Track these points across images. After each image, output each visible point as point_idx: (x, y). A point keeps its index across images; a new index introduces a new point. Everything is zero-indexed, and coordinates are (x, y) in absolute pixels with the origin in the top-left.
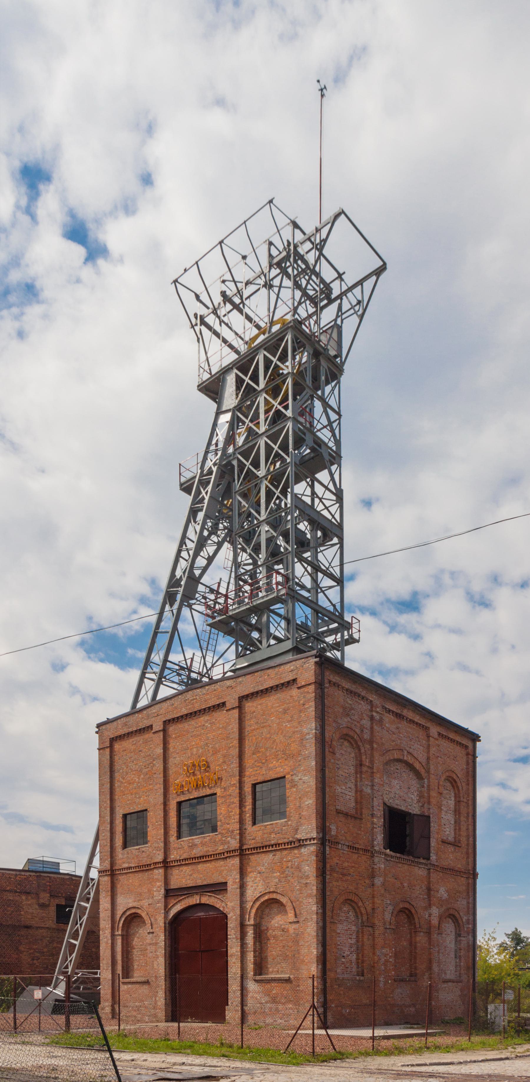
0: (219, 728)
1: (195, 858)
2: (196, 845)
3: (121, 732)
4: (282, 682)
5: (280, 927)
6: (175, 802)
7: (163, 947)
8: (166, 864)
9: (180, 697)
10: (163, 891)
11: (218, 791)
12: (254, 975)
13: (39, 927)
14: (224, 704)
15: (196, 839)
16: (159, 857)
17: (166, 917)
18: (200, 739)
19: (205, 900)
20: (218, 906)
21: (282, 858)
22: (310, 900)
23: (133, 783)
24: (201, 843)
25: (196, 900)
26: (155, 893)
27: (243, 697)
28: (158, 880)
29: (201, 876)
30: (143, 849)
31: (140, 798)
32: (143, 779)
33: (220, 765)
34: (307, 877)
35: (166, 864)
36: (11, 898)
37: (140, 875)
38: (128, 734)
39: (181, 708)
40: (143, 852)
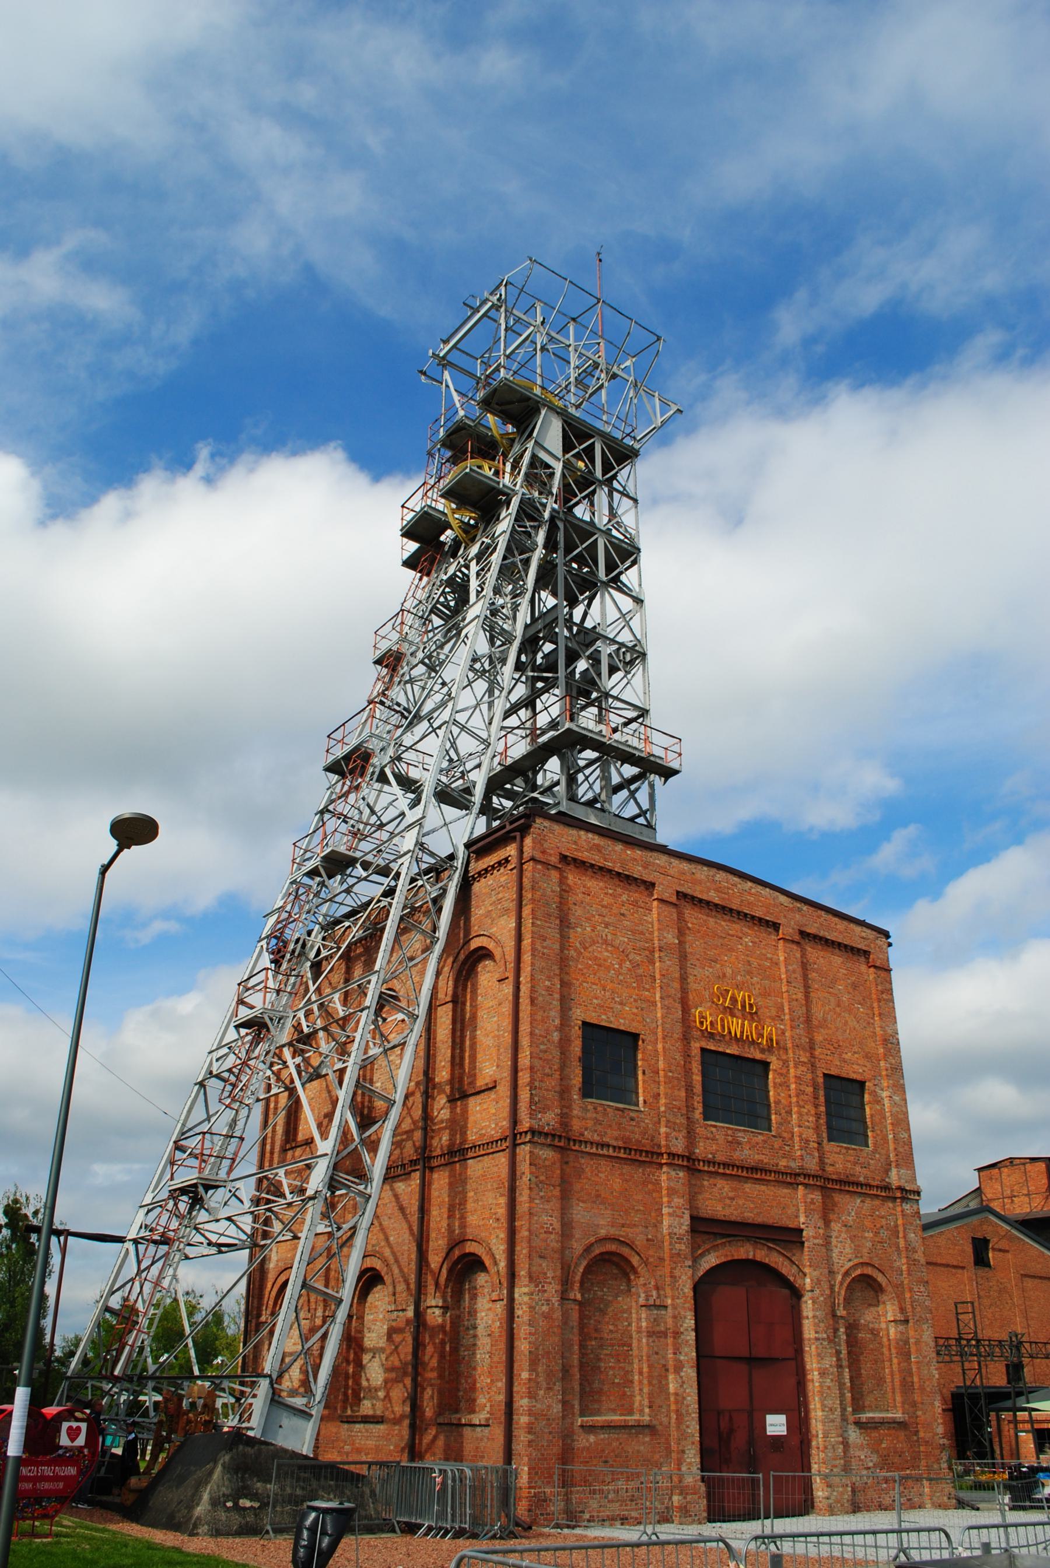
1: (742, 1168)
3: (585, 856)
7: (693, 1342)
10: (686, 1220)
11: (775, 1064)
14: (776, 926)
15: (740, 1130)
19: (761, 1255)
20: (784, 1271)
23: (608, 969)
25: (748, 1252)
30: (632, 1114)
37: (627, 1169)
38: (601, 868)
39: (709, 890)
40: (632, 1119)
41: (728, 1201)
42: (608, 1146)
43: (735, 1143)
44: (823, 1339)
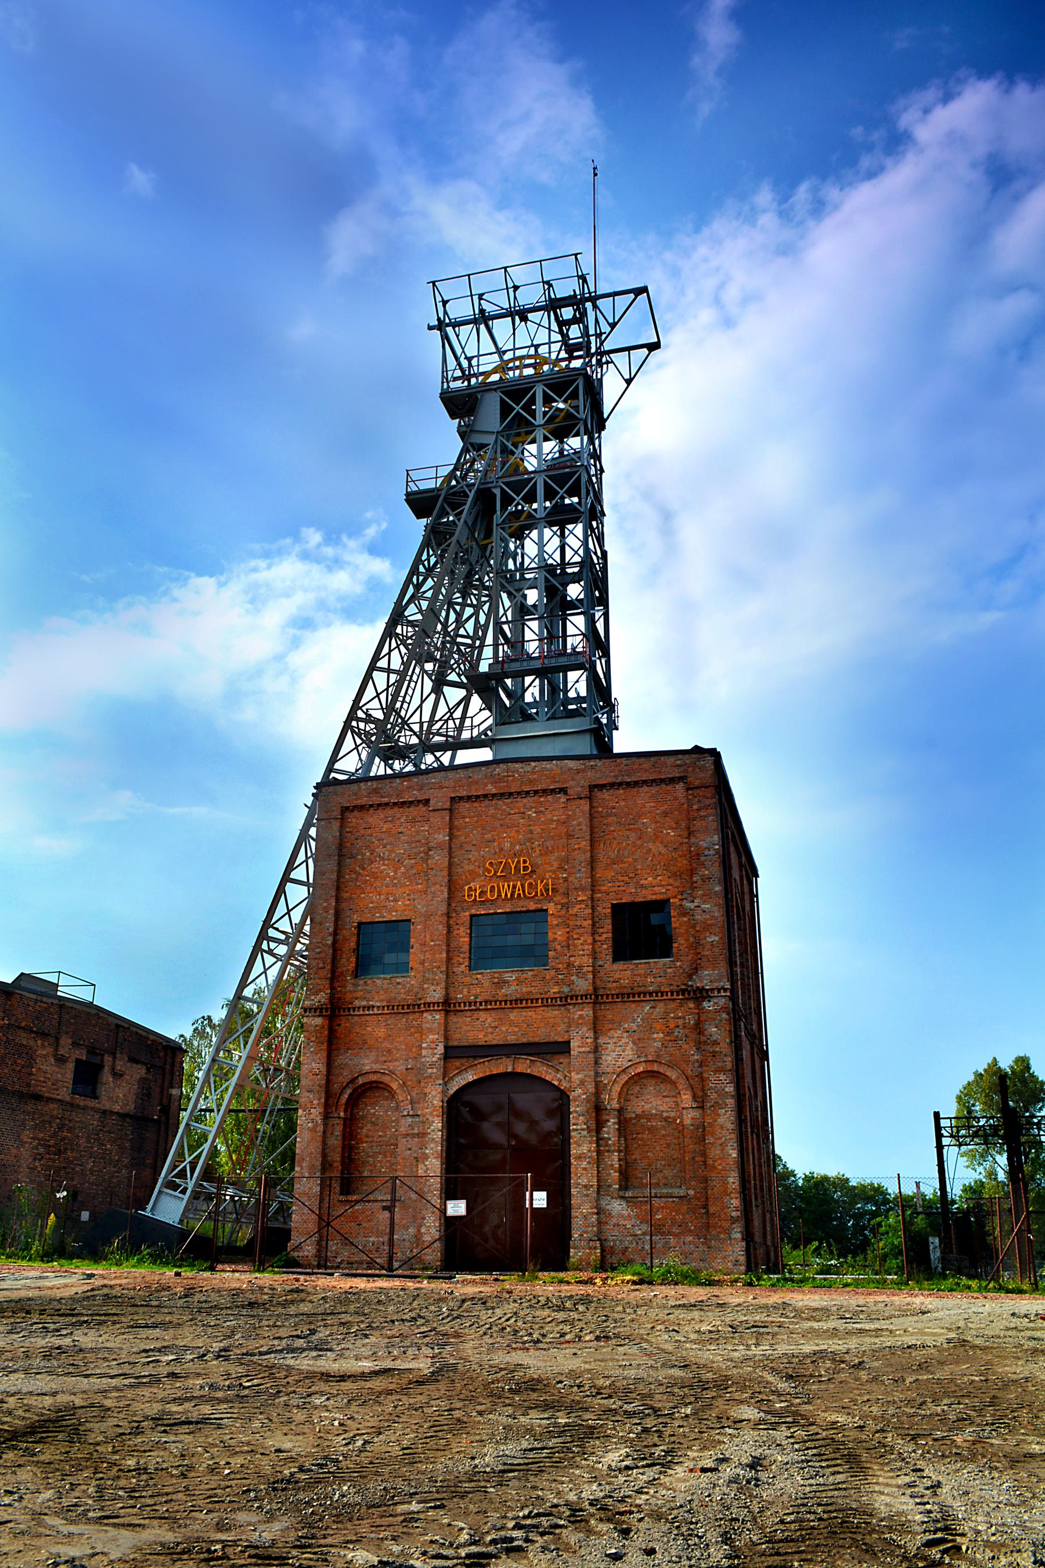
0: (552, 821)
2: (505, 982)
4: (663, 777)
5: (661, 1115)
6: (467, 914)
8: (448, 1006)
9: (483, 769)
10: (441, 1049)
11: (552, 908)
12: (620, 1189)
13: (51, 1099)
14: (563, 791)
16: (436, 994)
17: (444, 1092)
18: (517, 831)
19: (523, 1066)
21: (667, 1013)
22: (722, 1077)
24: (517, 979)
26: (424, 1052)
27: (596, 786)
28: (430, 1031)
29: (516, 1029)
31: (396, 901)
32: (403, 873)
33: (554, 872)
34: (716, 1043)
35: (448, 1006)
36: (25, 1043)
38: (379, 805)
41: (490, 1030)
42: (373, 1007)
43: (502, 983)
44: (583, 1130)
